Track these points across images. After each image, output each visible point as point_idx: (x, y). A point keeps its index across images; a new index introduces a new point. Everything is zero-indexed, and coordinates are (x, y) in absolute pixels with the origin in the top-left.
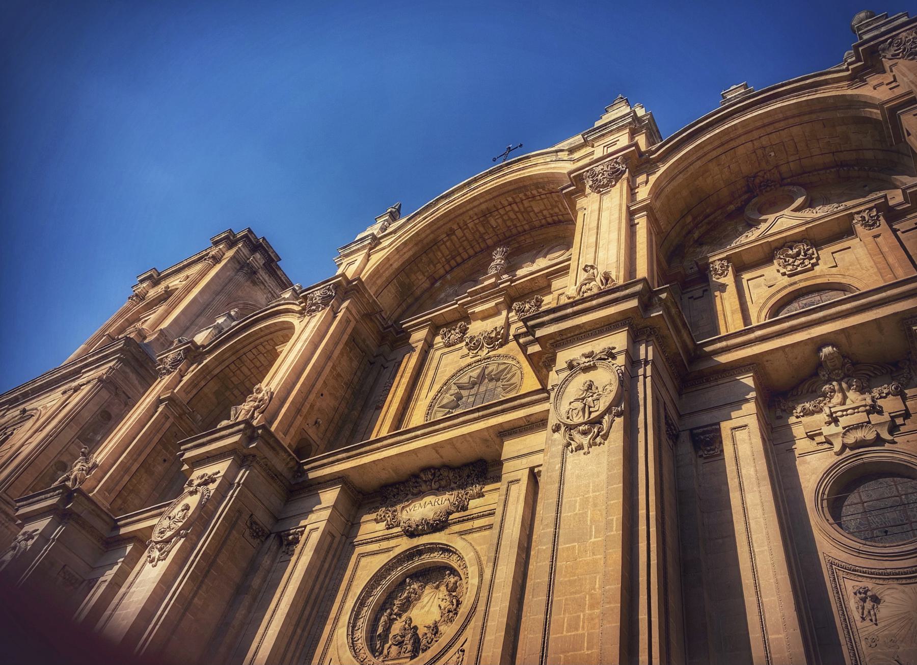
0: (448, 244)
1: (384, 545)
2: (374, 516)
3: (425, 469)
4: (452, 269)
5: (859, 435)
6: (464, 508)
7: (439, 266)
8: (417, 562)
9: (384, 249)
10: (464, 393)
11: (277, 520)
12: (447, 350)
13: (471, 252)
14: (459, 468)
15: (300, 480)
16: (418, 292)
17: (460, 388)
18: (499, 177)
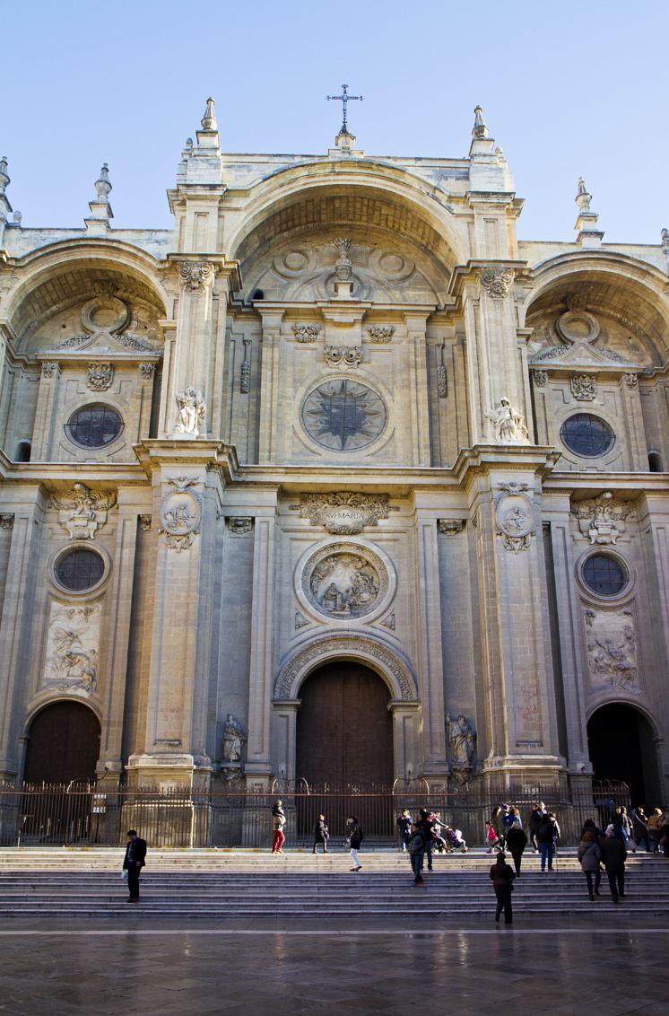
0: (289, 211)
1: (311, 535)
2: (298, 512)
3: (343, 492)
4: (282, 231)
5: (605, 539)
6: (376, 525)
7: (272, 228)
8: (337, 551)
9: (237, 210)
10: (328, 401)
11: (222, 506)
12: (300, 345)
13: (304, 220)
14: (369, 495)
15: (240, 479)
16: (249, 253)
17: (324, 396)
18: (368, 175)
